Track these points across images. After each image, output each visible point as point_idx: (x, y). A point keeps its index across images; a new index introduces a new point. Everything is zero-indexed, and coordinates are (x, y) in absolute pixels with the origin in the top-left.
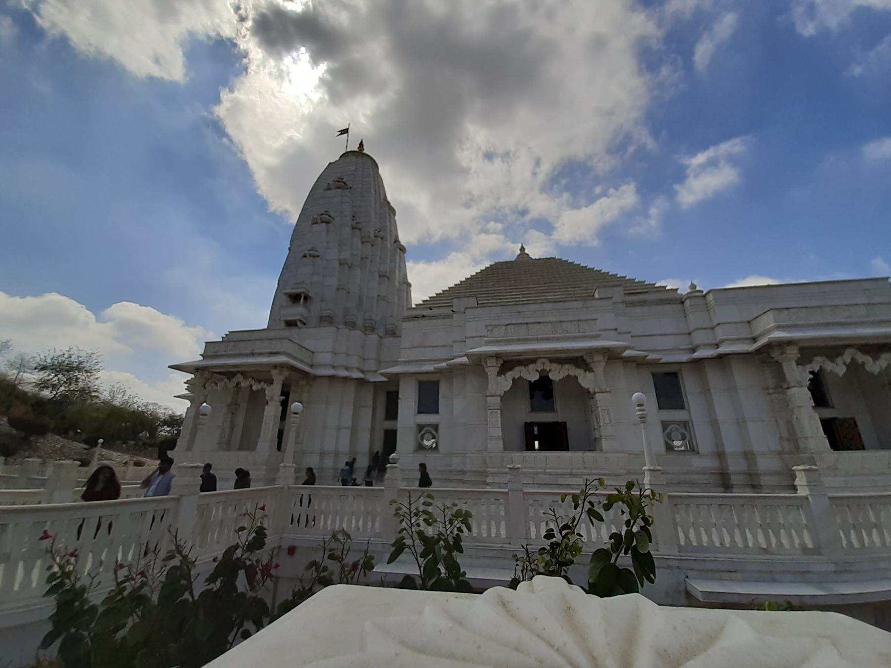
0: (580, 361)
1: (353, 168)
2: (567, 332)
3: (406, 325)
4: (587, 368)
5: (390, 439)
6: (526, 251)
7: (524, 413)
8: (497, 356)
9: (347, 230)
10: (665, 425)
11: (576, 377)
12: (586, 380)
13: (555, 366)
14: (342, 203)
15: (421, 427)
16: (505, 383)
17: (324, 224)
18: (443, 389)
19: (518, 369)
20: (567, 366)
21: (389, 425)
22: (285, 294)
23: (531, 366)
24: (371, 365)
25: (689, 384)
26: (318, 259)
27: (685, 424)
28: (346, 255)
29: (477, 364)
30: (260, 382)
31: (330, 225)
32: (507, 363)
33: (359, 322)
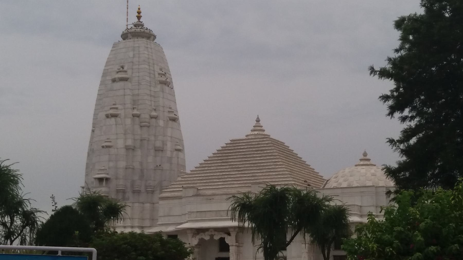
1: (131, 54)
2: (222, 217)
3: (161, 202)
4: (229, 234)
6: (261, 123)
8: (191, 229)
9: (128, 121)
11: (224, 238)
13: (216, 233)
14: (125, 95)
17: (113, 119)
19: (202, 234)
20: (221, 233)
22: (95, 178)
23: (207, 233)
24: (147, 223)
26: (111, 149)
28: (129, 142)
31: (118, 119)
33: (143, 189)
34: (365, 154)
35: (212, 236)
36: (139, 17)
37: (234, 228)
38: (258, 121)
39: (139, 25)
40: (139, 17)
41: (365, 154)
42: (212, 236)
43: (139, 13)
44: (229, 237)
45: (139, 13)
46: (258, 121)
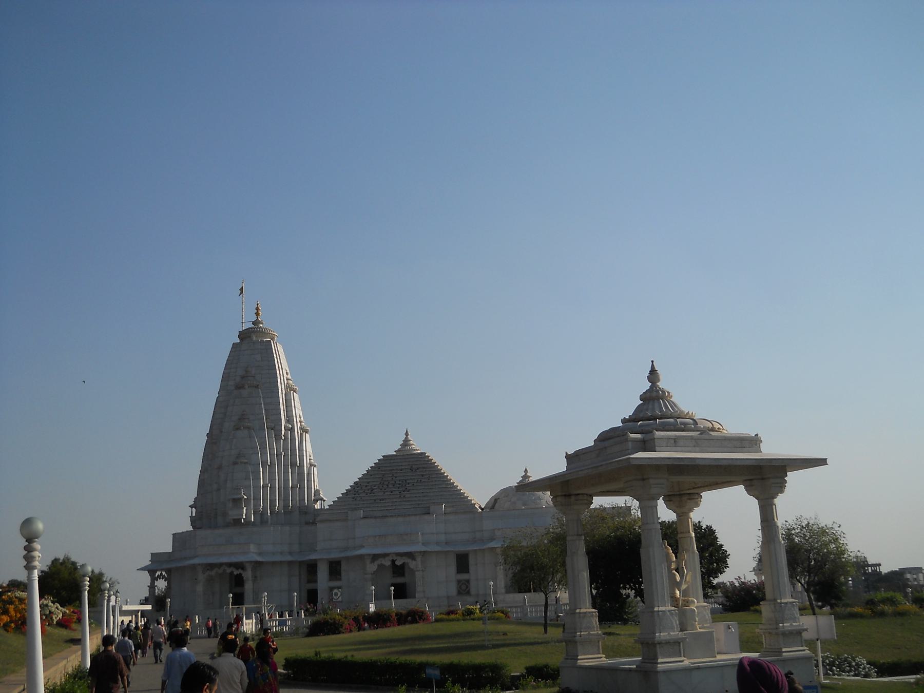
0: (410, 555)
5: (312, 597)
7: (388, 578)
10: (459, 582)
12: (412, 564)
13: (398, 558)
15: (331, 589)
16: (372, 567)
18: (344, 567)
21: (311, 586)
23: (387, 558)
25: (472, 561)
27: (468, 581)
29: (361, 557)
30: (237, 569)
32: (375, 557)
34: (526, 471)
35: (393, 561)
36: (257, 314)
37: (420, 552)
38: (407, 434)
39: (256, 323)
40: (257, 314)
41: (526, 471)
42: (393, 561)
43: (257, 309)
44: (414, 562)
45: (257, 309)
46: (407, 434)
